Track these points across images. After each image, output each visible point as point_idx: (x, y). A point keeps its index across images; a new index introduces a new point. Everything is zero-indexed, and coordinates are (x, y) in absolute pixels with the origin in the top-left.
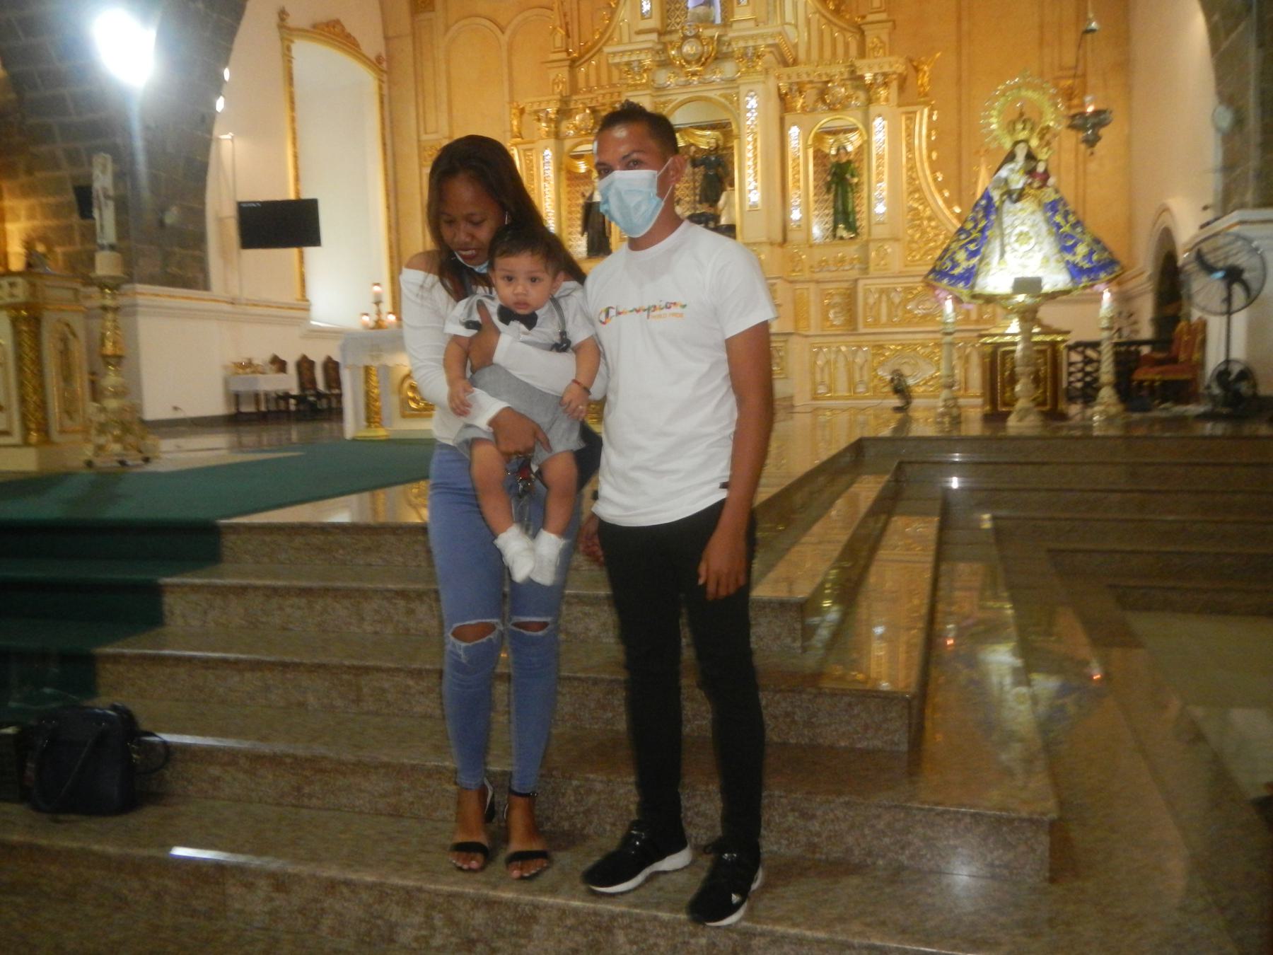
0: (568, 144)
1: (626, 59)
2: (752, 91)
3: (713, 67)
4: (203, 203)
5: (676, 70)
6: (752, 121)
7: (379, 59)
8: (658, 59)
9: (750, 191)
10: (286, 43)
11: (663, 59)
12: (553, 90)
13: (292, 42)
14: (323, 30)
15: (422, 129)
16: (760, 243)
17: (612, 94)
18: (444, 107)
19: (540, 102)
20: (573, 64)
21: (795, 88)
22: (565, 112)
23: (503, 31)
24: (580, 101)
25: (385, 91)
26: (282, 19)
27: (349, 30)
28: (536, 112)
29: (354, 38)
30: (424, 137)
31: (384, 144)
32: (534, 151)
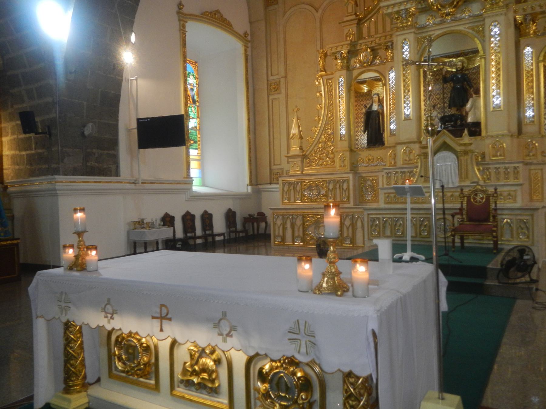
0: (355, 73)
1: (396, 9)
2: (496, 21)
3: (463, 8)
4: (117, 121)
5: (434, 14)
6: (496, 44)
7: (246, 34)
8: (420, 6)
9: (494, 96)
10: (182, 23)
11: (424, 6)
12: (346, 39)
13: (187, 22)
14: (207, 15)
15: (270, 73)
16: (503, 136)
17: (386, 36)
18: (282, 59)
19: (337, 47)
20: (360, 22)
21: (529, 18)
22: (353, 52)
23: (317, 11)
24: (363, 45)
25: (249, 53)
26: (180, 9)
27: (225, 16)
28: (334, 54)
29: (229, 21)
30: (271, 78)
31: (247, 83)
32: (333, 79)
